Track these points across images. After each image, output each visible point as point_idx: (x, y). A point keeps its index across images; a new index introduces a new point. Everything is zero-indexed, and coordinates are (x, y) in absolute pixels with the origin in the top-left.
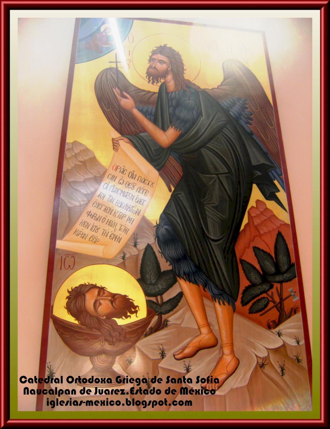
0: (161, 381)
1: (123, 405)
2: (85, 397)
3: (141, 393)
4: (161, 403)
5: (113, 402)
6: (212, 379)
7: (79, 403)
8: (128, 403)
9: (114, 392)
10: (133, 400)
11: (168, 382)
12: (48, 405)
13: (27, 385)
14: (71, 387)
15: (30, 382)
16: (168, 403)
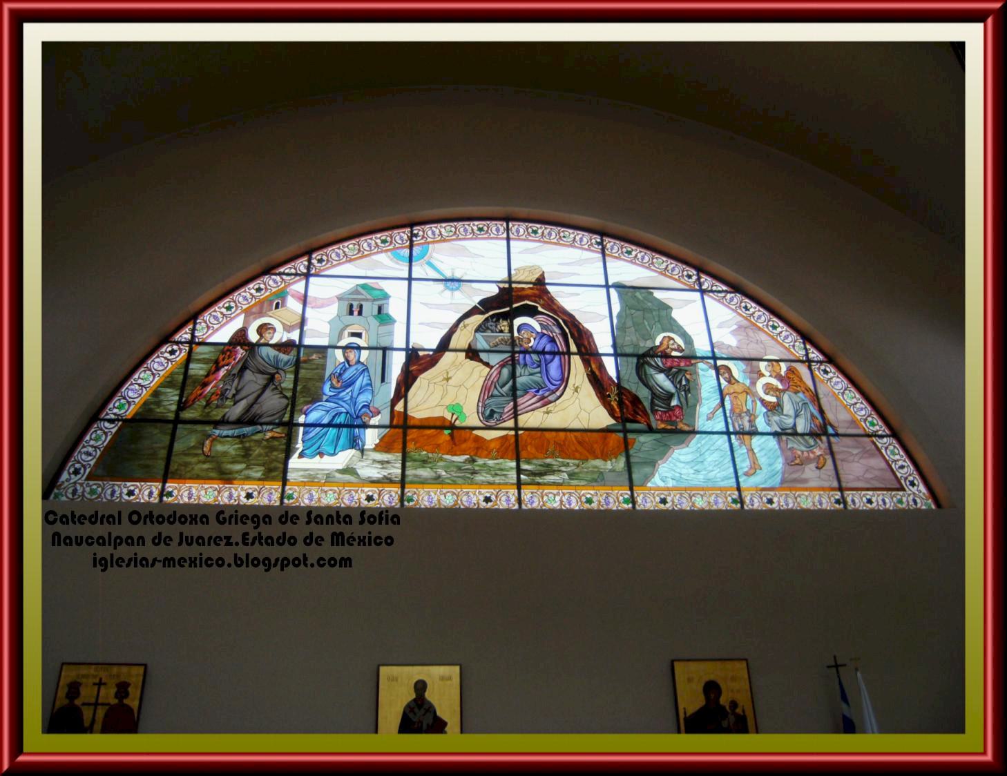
0: (297, 521)
1: (229, 565)
2: (162, 552)
3: (261, 544)
4: (296, 562)
5: (211, 559)
6: (387, 516)
7: (150, 562)
8: (238, 562)
9: (212, 541)
10: (247, 555)
11: (308, 523)
12: (95, 566)
13: (58, 527)
14: (136, 531)
15: (62, 522)
16: (309, 562)
